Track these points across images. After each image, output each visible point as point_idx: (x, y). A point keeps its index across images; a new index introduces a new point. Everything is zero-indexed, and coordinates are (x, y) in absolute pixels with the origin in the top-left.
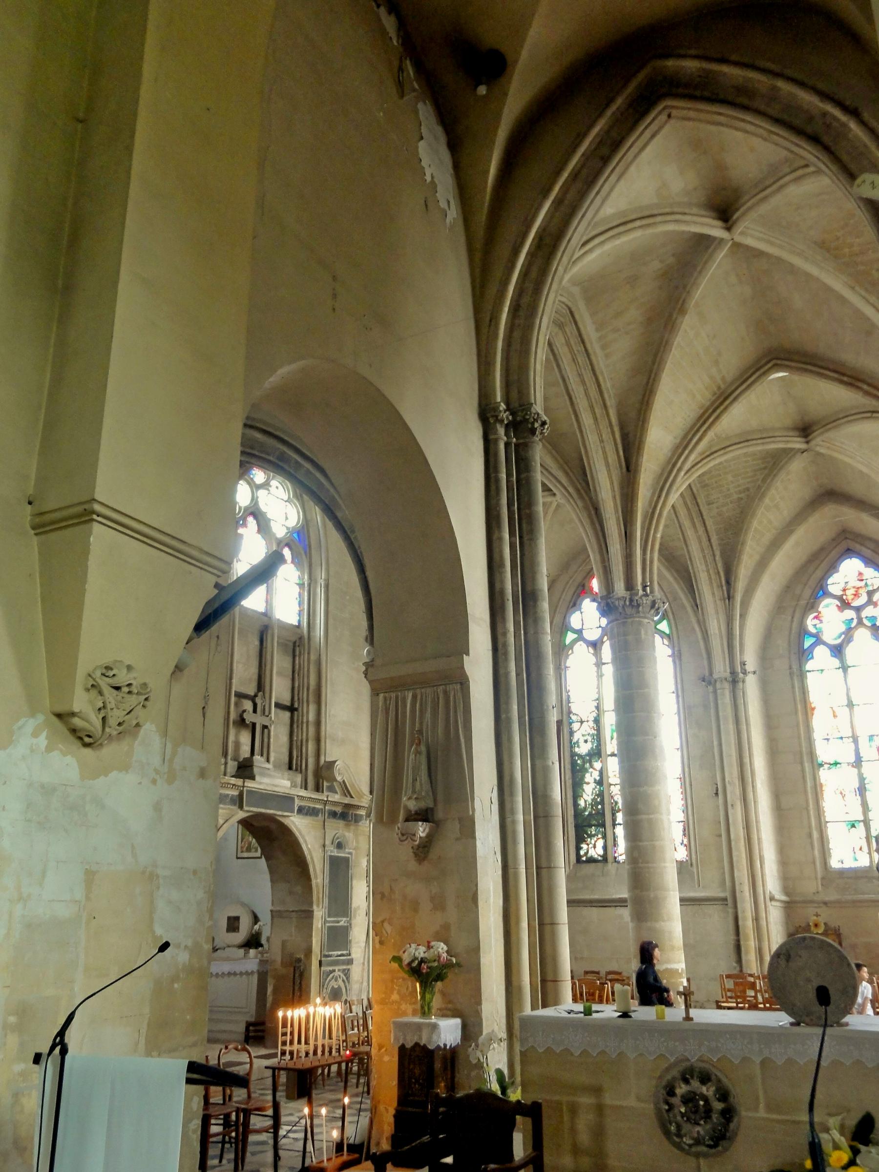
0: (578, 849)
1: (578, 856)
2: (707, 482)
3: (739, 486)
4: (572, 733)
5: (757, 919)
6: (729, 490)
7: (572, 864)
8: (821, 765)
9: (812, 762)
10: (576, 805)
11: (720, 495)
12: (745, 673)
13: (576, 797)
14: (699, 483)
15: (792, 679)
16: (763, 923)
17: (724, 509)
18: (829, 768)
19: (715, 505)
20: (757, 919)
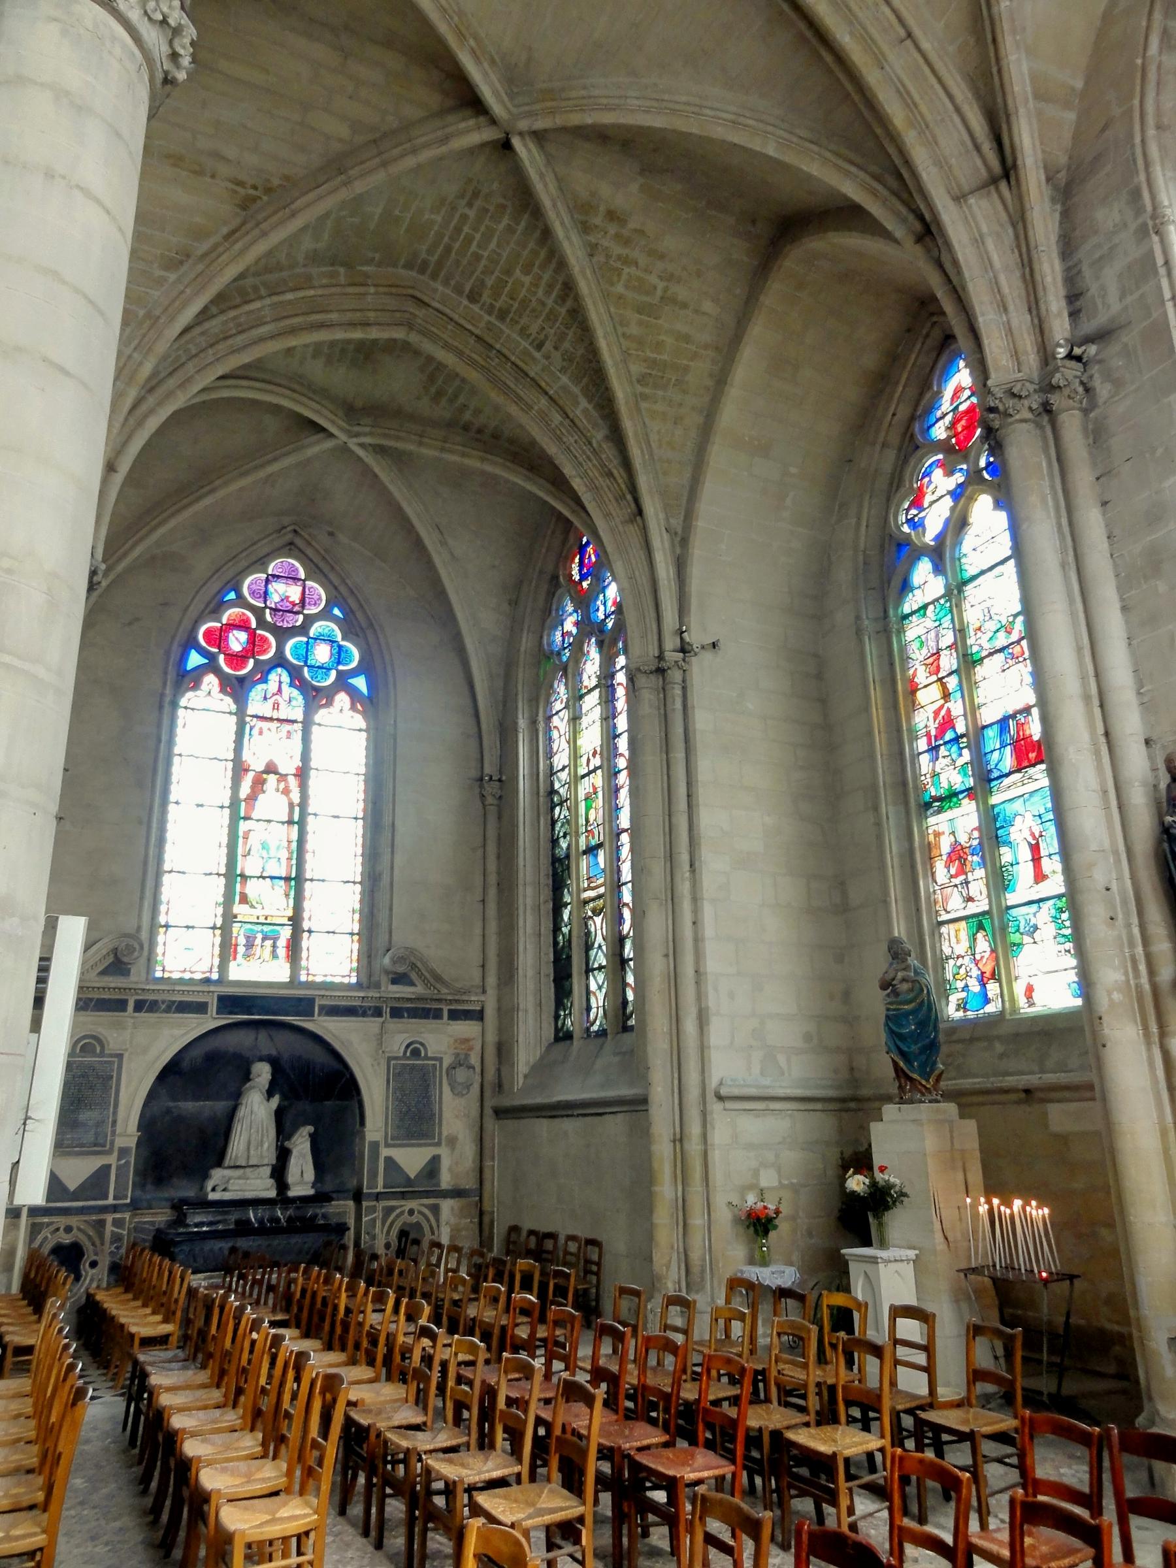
0: (557, 1017)
1: (557, 1030)
2: (498, 305)
3: (550, 286)
4: (553, 822)
5: (679, 1140)
6: (543, 304)
7: (545, 1044)
8: (928, 805)
9: (906, 803)
10: (556, 943)
11: (540, 321)
12: (684, 649)
13: (556, 929)
14: (490, 314)
15: (861, 642)
16: (694, 1146)
17: (566, 345)
18: (940, 811)
19: (548, 346)
20: (679, 1140)
